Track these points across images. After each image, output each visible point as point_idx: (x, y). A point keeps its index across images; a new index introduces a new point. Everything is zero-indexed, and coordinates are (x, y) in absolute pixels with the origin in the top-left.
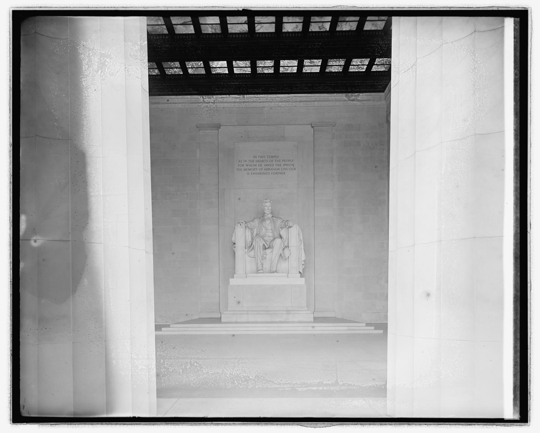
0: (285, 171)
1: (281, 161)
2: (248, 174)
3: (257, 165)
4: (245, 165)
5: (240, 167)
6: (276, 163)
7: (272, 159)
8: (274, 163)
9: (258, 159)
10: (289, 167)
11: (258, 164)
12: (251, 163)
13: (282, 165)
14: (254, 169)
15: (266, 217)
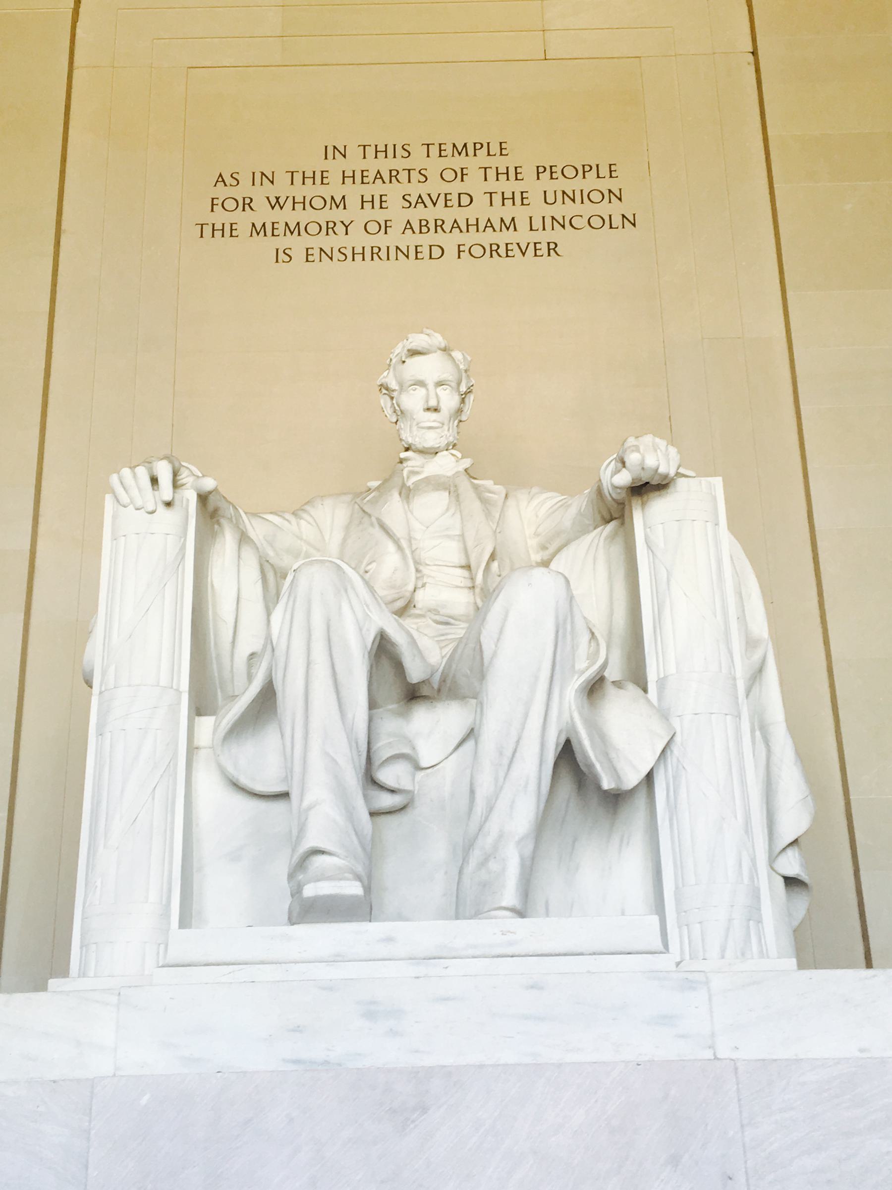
0: (558, 235)
1: (528, 172)
2: (283, 256)
3: (353, 202)
4: (260, 203)
5: (220, 217)
6: (492, 185)
7: (458, 162)
8: (474, 184)
9: (354, 162)
10: (588, 209)
11: (353, 192)
12: (309, 190)
13: (535, 197)
14: (330, 228)
15: (410, 483)
